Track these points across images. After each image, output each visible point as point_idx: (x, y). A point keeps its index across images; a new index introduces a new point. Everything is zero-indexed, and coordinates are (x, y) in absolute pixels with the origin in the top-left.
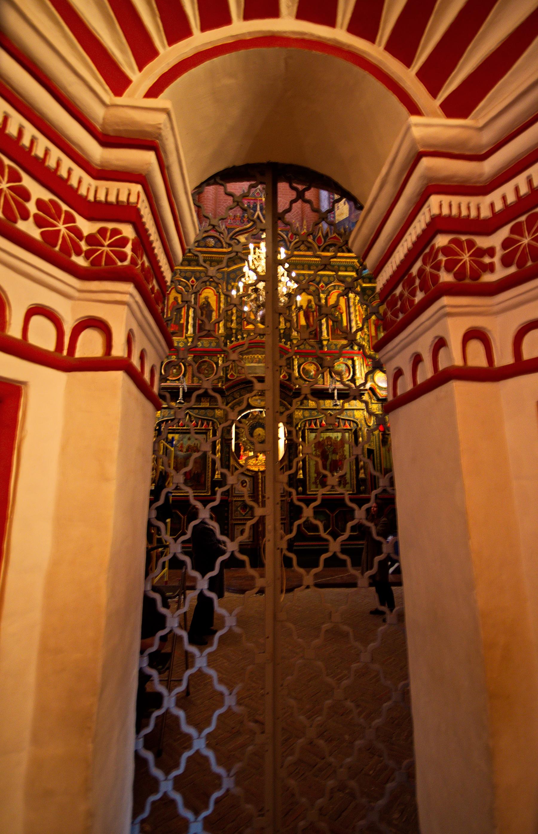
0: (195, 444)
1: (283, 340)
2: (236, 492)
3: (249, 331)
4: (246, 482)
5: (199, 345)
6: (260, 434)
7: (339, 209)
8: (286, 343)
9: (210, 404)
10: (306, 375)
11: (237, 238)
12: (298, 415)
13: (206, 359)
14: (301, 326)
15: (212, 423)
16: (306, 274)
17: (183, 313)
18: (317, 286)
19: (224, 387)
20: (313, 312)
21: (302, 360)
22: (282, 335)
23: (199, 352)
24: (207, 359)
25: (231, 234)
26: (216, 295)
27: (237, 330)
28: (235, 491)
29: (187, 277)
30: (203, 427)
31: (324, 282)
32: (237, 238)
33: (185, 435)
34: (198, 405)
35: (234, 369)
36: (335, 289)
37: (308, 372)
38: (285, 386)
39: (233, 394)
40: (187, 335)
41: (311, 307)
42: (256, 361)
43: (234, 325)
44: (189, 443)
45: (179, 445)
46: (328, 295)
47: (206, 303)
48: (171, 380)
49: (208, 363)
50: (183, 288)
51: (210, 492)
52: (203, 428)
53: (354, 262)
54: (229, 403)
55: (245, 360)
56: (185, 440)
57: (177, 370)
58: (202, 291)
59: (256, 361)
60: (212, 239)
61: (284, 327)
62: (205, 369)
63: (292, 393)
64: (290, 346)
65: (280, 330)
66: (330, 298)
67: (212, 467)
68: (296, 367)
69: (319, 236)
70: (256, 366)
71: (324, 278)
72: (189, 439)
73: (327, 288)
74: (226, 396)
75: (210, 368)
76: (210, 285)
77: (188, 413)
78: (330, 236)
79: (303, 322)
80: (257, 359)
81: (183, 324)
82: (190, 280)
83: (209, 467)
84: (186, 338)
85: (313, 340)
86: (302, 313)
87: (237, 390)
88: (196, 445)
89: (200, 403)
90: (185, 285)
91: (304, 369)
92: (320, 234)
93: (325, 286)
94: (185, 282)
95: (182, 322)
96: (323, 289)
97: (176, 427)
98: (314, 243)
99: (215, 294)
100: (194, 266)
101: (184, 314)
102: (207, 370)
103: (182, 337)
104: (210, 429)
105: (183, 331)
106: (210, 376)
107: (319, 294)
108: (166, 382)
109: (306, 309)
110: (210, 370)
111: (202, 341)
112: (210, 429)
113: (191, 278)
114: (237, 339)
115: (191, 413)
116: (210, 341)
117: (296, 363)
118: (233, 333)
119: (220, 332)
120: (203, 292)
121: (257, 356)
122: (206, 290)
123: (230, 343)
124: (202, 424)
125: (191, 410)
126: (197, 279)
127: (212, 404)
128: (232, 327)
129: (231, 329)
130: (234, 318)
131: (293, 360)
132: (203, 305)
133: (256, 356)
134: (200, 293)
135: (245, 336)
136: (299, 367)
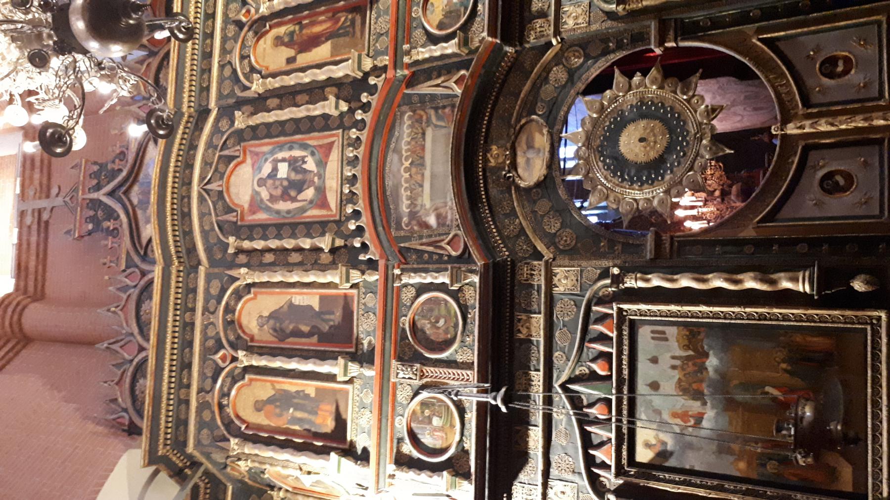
0: (674, 367)
1: (364, 97)
2: (877, 212)
3: (341, 201)
4: (829, 175)
5: (370, 343)
6: (641, 140)
8: (372, 90)
9: (535, 313)
10: (460, 16)
11: (144, 242)
12: (576, 18)
13: (405, 322)
14: (332, 56)
15: (597, 304)
17: (293, 389)
18: (246, 28)
19: (480, 263)
20: (301, 29)
21: (418, 34)
22: (353, 105)
23: (387, 344)
24: (407, 319)
25: (136, 259)
26: (255, 295)
27: (339, 234)
28: (873, 217)
29: (213, 375)
30: (610, 334)
32: (144, 242)
33: (639, 401)
34: (539, 351)
35: (438, 238)
37: (450, 12)
38: (483, 71)
39: (508, 237)
40: (339, 379)
41: (292, 34)
42: (417, 173)
43: (325, 243)
44: (669, 386)
45: (677, 424)
47: (272, 322)
48: (462, 434)
49: (416, 317)
51: (875, 314)
52: (614, 335)
54: (535, 247)
55: (416, 205)
56: (657, 401)
57: (434, 414)
58: (244, 332)
59: (417, 173)
61: (332, 99)
62: (434, 325)
63: (509, 49)
64: (378, 77)
65: (342, 114)
67: (763, 305)
68: (437, 51)
70: (433, 176)
71: (231, 15)
72: (654, 386)
74: (512, 261)
75: (431, 310)
76: (233, 311)
77: (563, 386)
79: (323, 51)
80: (414, 170)
81: (318, 390)
83: (762, 317)
84: (350, 381)
85: (368, 12)
86: (304, 59)
87: (496, 227)
88: (678, 363)
89: (531, 342)
91: (440, 26)
94: (223, 381)
95: (311, 392)
96: (253, 11)
97: (611, 432)
99: (251, 299)
101: (296, 384)
102: (437, 322)
103: (346, 392)
104: (620, 310)
105: (334, 391)
106: (453, 312)
108: (466, 453)
109: (296, 47)
110: (436, 313)
111: (362, 336)
112: (620, 310)
113: (215, 362)
114: (360, 230)
115: (564, 377)
116: (361, 312)
117: (423, 53)
118: (346, 245)
119: (337, 280)
120: (247, 330)
121: (406, 172)
122: (244, 321)
123: (366, 253)
124: (602, 338)
125: (555, 376)
126: (221, 347)
127: (535, 307)
128: (329, 247)
129: (333, 250)
130: (306, 244)
131: (417, 63)
132: (275, 330)
133: (407, 175)
134: (248, 339)
135: (349, 210)
136: (433, 40)
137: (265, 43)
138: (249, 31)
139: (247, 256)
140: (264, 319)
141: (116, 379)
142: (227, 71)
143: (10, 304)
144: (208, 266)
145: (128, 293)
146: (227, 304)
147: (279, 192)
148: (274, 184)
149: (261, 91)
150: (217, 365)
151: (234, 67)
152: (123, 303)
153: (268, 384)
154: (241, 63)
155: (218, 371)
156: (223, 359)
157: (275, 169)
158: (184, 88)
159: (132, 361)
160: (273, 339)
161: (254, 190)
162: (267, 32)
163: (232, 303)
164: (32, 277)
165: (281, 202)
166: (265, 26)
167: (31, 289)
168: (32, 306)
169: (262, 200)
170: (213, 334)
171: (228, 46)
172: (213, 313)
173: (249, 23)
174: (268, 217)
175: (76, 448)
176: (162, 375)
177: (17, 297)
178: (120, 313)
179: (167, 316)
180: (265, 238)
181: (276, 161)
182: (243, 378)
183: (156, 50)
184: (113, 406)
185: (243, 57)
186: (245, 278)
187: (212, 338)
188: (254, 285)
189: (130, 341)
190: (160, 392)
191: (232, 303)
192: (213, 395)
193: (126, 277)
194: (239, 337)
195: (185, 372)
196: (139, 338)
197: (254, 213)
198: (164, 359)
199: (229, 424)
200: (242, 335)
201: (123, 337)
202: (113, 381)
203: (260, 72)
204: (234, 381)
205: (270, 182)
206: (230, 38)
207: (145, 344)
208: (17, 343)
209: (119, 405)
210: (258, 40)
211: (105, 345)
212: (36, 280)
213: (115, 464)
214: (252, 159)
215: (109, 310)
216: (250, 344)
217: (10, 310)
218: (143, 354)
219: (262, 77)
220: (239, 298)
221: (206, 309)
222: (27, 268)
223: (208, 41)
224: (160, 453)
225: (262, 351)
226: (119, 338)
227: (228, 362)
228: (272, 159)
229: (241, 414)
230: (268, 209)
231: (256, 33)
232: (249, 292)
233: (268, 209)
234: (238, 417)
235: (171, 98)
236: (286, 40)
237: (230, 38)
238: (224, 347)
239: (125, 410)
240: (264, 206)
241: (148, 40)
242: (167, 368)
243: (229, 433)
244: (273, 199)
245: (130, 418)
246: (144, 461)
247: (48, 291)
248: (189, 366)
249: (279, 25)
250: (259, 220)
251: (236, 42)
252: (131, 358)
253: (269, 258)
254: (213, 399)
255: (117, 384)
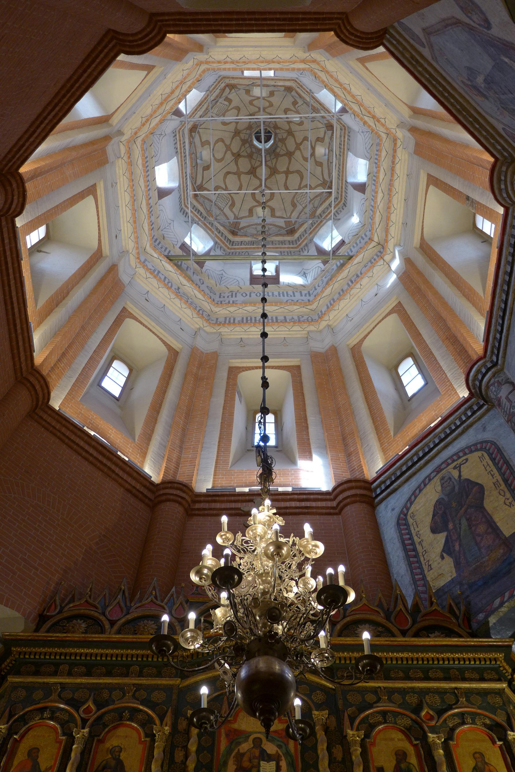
7: (431, 569)
16: (380, 687)
18: (414, 716)
31: (430, 707)
36: (463, 723)
46: (450, 737)
47: (113, 763)
50: (58, 726)
53: (495, 660)
60: (151, 621)
66: (457, 745)
69: (398, 609)
71: (428, 698)
73: (441, 720)
76: (131, 719)
78: (423, 611)
82: (79, 707)
90: (66, 718)
92: (400, 606)
93: (436, 717)
96: (433, 723)
98: (389, 625)
100: (100, 676)
107: (426, 737)
113: (87, 701)
126: (99, 706)
132: (104, 768)
137: (399, 740)
138: (412, 720)
139: (185, 730)
140: (117, 754)
141: (91, 601)
142: (370, 698)
143: (184, 492)
144: (180, 686)
145: (165, 607)
146: (141, 710)
147: (246, 764)
148: (255, 757)
149: (350, 738)
150: (84, 703)
151: (375, 705)
152: (158, 602)
153: (52, 763)
154: (378, 712)
155: (75, 704)
156: (88, 710)
157: (269, 758)
158: (353, 652)
159: (104, 614)
160: (96, 764)
161: (251, 734)
162: (411, 742)
163: (140, 717)
164: (207, 506)
165: (235, 767)
166: (416, 739)
167: (197, 506)
168: (181, 509)
169: (239, 744)
170: (114, 697)
171: (396, 696)
172: (134, 696)
173: (418, 719)
174: (221, 752)
175: (37, 569)
176: (83, 647)
177: (190, 496)
178: (150, 599)
179: (137, 649)
180: (198, 752)
181: (277, 759)
182: (64, 734)
183: (392, 619)
184: (71, 596)
185: (384, 714)
186: (160, 731)
187: (110, 696)
188: (153, 741)
189: (122, 611)
190: (69, 647)
191: (140, 717)
192: (56, 702)
193: (181, 603)
194: (105, 726)
195: (83, 669)
196: (123, 620)
197: (227, 736)
198: (98, 648)
199: (24, 720)
200: (107, 730)
201: (128, 604)
202: (90, 597)
203: (367, 735)
204: (63, 724)
205: (257, 753)
206: (404, 699)
207: (116, 627)
208: (150, 500)
209: (67, 604)
210: (401, 731)
211: (123, 587)
212: (205, 509)
213: (12, 608)
214: (282, 730)
215: (154, 588)
216: (96, 739)
217: (178, 492)
218: (107, 626)
219: (363, 740)
220: (143, 725)
221: (138, 687)
222: (215, 501)
223: (401, 674)
224: (13, 649)
225: (85, 753)
226: (128, 600)
227: (82, 716)
228: (281, 753)
229: (31, 733)
230: (229, 751)
231: (409, 729)
232: (147, 736)
233: (229, 751)
234: (29, 729)
235: (341, 641)
236: (403, 766)
237: (404, 699)
238: (98, 709)
239: (60, 612)
240: (233, 747)
241: (401, 609)
242: (91, 651)
243: (15, 721)
244: (240, 756)
245: (52, 617)
246: (7, 635)
247: (195, 519)
248: (89, 674)
249: (418, 756)
250: (219, 742)
251: (400, 706)
252: (107, 613)
253: (179, 755)
254: (51, 701)
255: (86, 601)
